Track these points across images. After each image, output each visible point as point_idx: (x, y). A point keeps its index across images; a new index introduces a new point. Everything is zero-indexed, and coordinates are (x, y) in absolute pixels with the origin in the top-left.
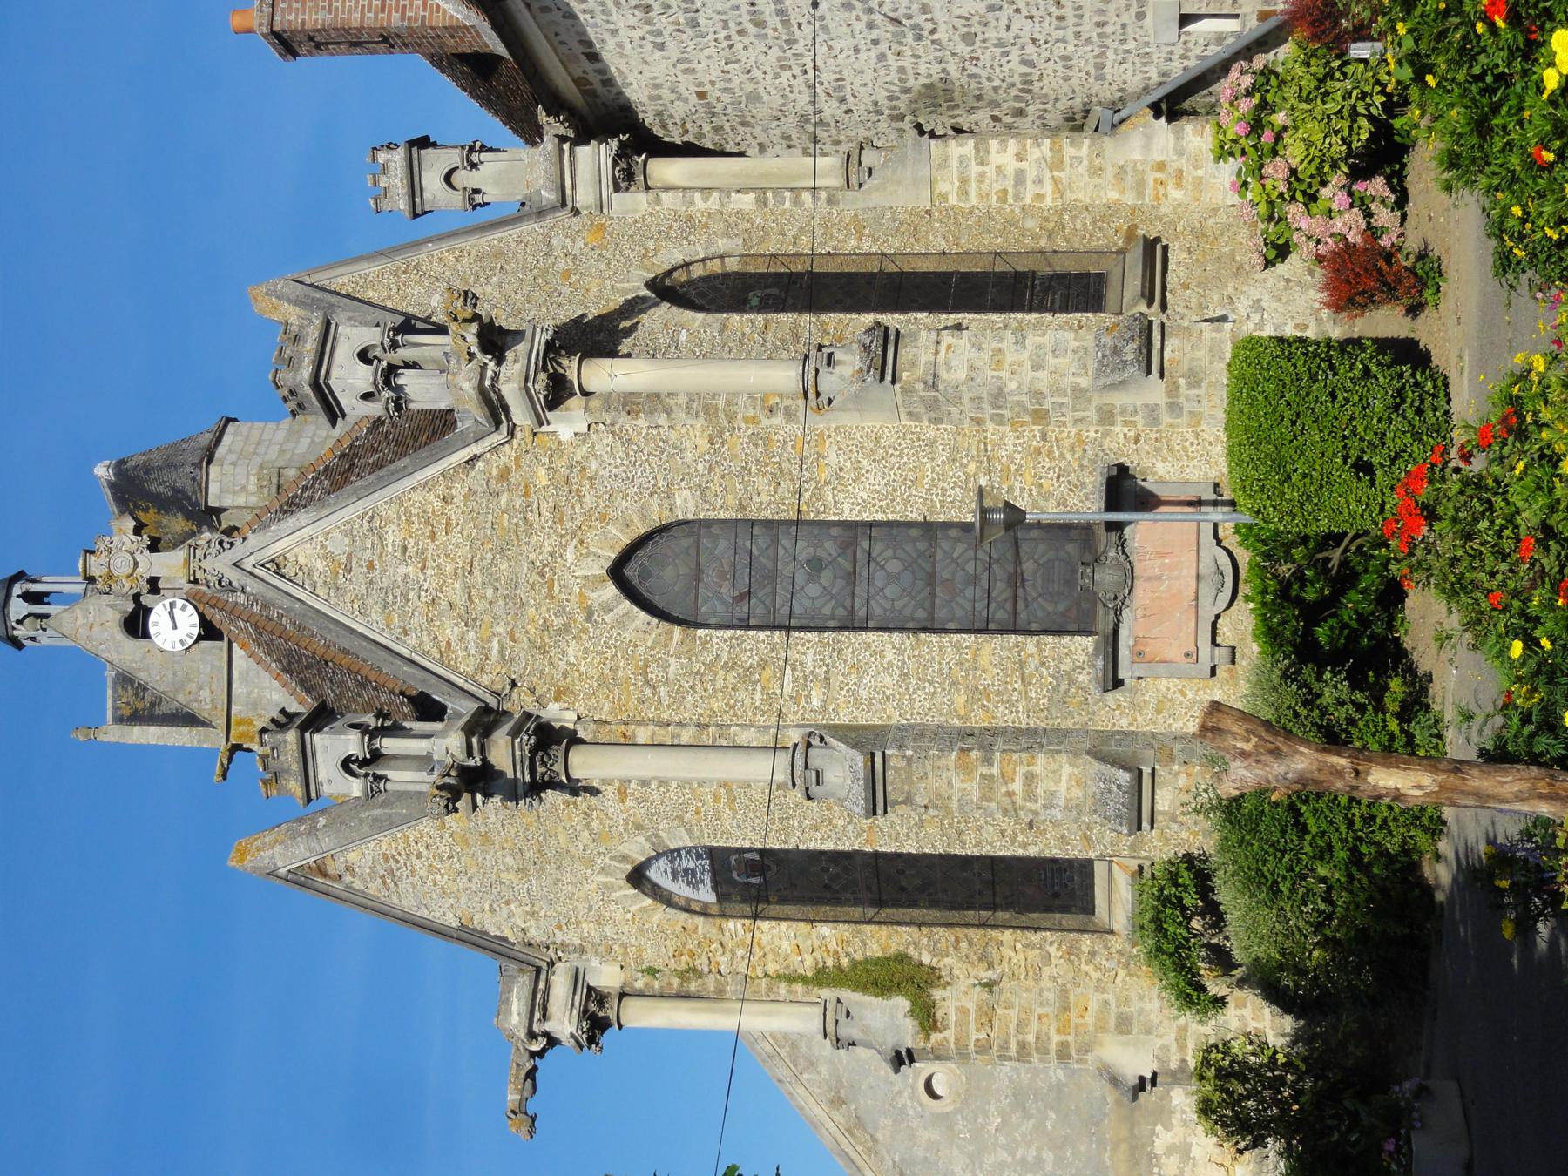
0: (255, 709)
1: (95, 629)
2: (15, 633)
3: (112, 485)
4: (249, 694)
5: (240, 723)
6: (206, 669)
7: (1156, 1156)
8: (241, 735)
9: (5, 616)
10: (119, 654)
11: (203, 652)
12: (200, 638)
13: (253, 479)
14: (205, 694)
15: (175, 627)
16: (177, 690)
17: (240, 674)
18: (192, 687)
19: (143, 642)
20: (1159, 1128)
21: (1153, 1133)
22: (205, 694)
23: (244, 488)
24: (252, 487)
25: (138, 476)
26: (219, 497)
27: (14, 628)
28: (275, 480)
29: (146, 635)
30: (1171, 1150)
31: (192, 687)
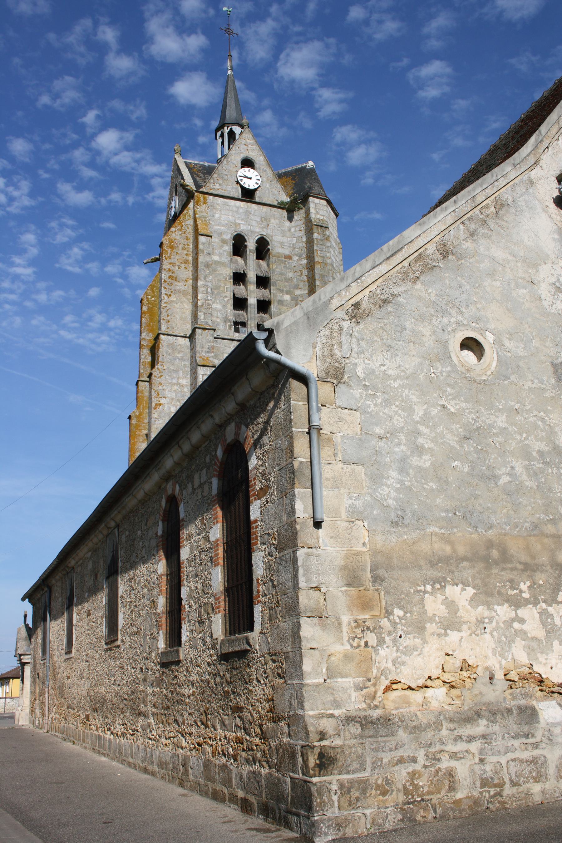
0: (211, 206)
1: (245, 146)
2: (226, 128)
3: (304, 168)
4: (218, 204)
5: (204, 198)
6: (229, 188)
7: (443, 587)
8: (198, 198)
9: (234, 124)
10: (235, 154)
11: (236, 188)
12: (243, 188)
13: (322, 217)
14: (217, 186)
15: (250, 178)
16: (219, 174)
17: (227, 202)
18: (221, 181)
19: (240, 165)
20: (470, 591)
21: (466, 584)
22: (217, 186)
23: (318, 213)
24: (318, 216)
25: (312, 176)
26: (313, 202)
27: (228, 127)
28: (324, 225)
29: (242, 167)
30: (450, 604)
31: (221, 181)
